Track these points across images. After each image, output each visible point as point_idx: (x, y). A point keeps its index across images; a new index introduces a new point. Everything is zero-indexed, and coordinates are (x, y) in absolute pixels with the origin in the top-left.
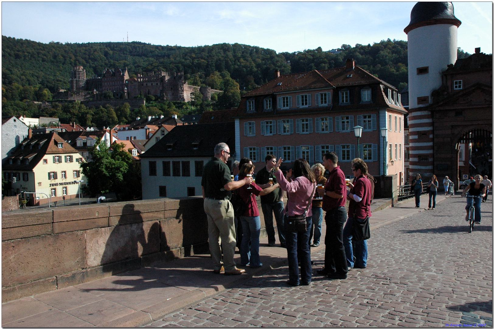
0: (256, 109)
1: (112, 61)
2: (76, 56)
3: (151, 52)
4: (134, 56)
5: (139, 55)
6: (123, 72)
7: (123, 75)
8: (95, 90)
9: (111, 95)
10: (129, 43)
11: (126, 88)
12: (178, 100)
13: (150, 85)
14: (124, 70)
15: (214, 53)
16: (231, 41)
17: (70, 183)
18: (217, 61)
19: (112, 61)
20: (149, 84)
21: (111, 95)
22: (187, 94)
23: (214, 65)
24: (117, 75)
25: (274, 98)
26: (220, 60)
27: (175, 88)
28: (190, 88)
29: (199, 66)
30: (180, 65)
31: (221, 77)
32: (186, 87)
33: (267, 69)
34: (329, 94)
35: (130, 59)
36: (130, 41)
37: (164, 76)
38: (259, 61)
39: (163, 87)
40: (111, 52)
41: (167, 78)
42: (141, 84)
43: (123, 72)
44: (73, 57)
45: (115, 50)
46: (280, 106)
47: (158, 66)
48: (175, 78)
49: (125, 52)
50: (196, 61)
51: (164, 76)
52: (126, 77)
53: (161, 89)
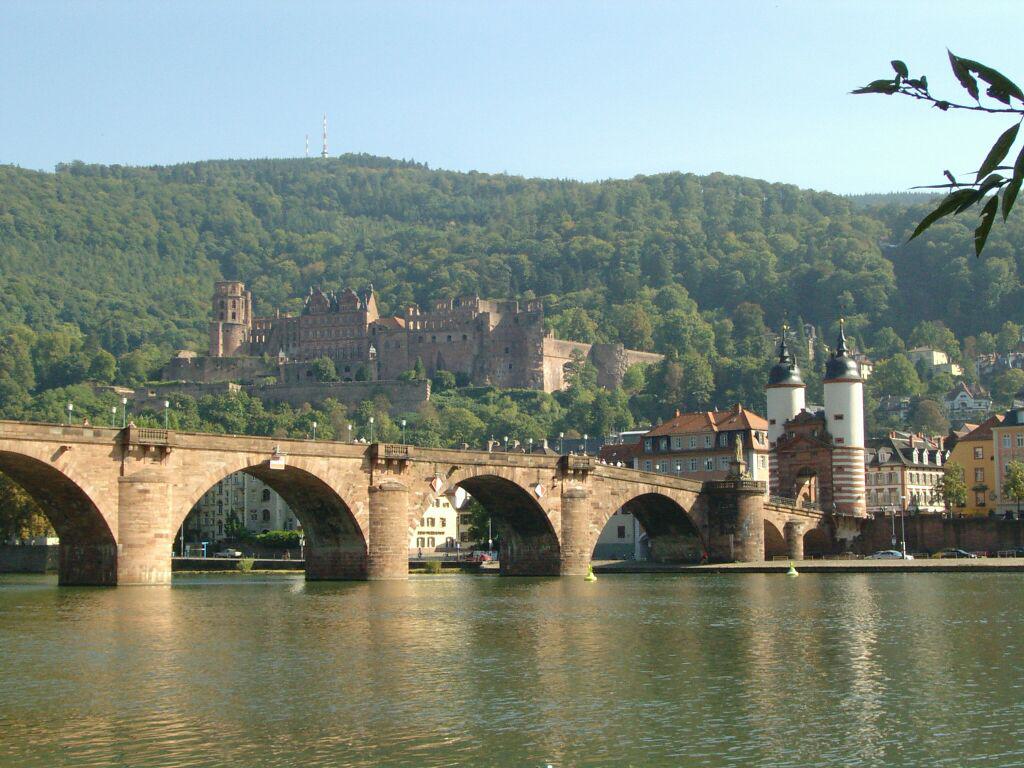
0: (653, 449)
1: (281, 232)
2: (160, 217)
3: (417, 199)
4: (357, 214)
5: (370, 213)
6: (363, 301)
7: (364, 309)
8: (282, 354)
9: (330, 366)
10: (332, 162)
11: (373, 350)
12: (525, 387)
13: (445, 340)
14: (364, 294)
15: (638, 213)
16: (699, 163)
17: (436, 533)
18: (648, 243)
19: (281, 232)
20: (441, 338)
21: (330, 366)
22: (553, 369)
23: (637, 257)
24: (345, 308)
25: (668, 438)
26: (657, 239)
27: (520, 351)
28: (561, 348)
29: (588, 261)
30: (524, 258)
31: (655, 308)
32: (549, 345)
33: (814, 275)
34: (712, 438)
35: (341, 222)
36: (335, 152)
37: (486, 315)
38: (791, 243)
39: (481, 345)
40: (276, 200)
41: (494, 321)
42: (416, 338)
43: (363, 301)
44: (155, 226)
45: (292, 193)
46: (675, 447)
47: (449, 262)
48: (516, 321)
49: (326, 200)
50: (576, 243)
51: (486, 315)
52: (372, 316)
53: (475, 351)
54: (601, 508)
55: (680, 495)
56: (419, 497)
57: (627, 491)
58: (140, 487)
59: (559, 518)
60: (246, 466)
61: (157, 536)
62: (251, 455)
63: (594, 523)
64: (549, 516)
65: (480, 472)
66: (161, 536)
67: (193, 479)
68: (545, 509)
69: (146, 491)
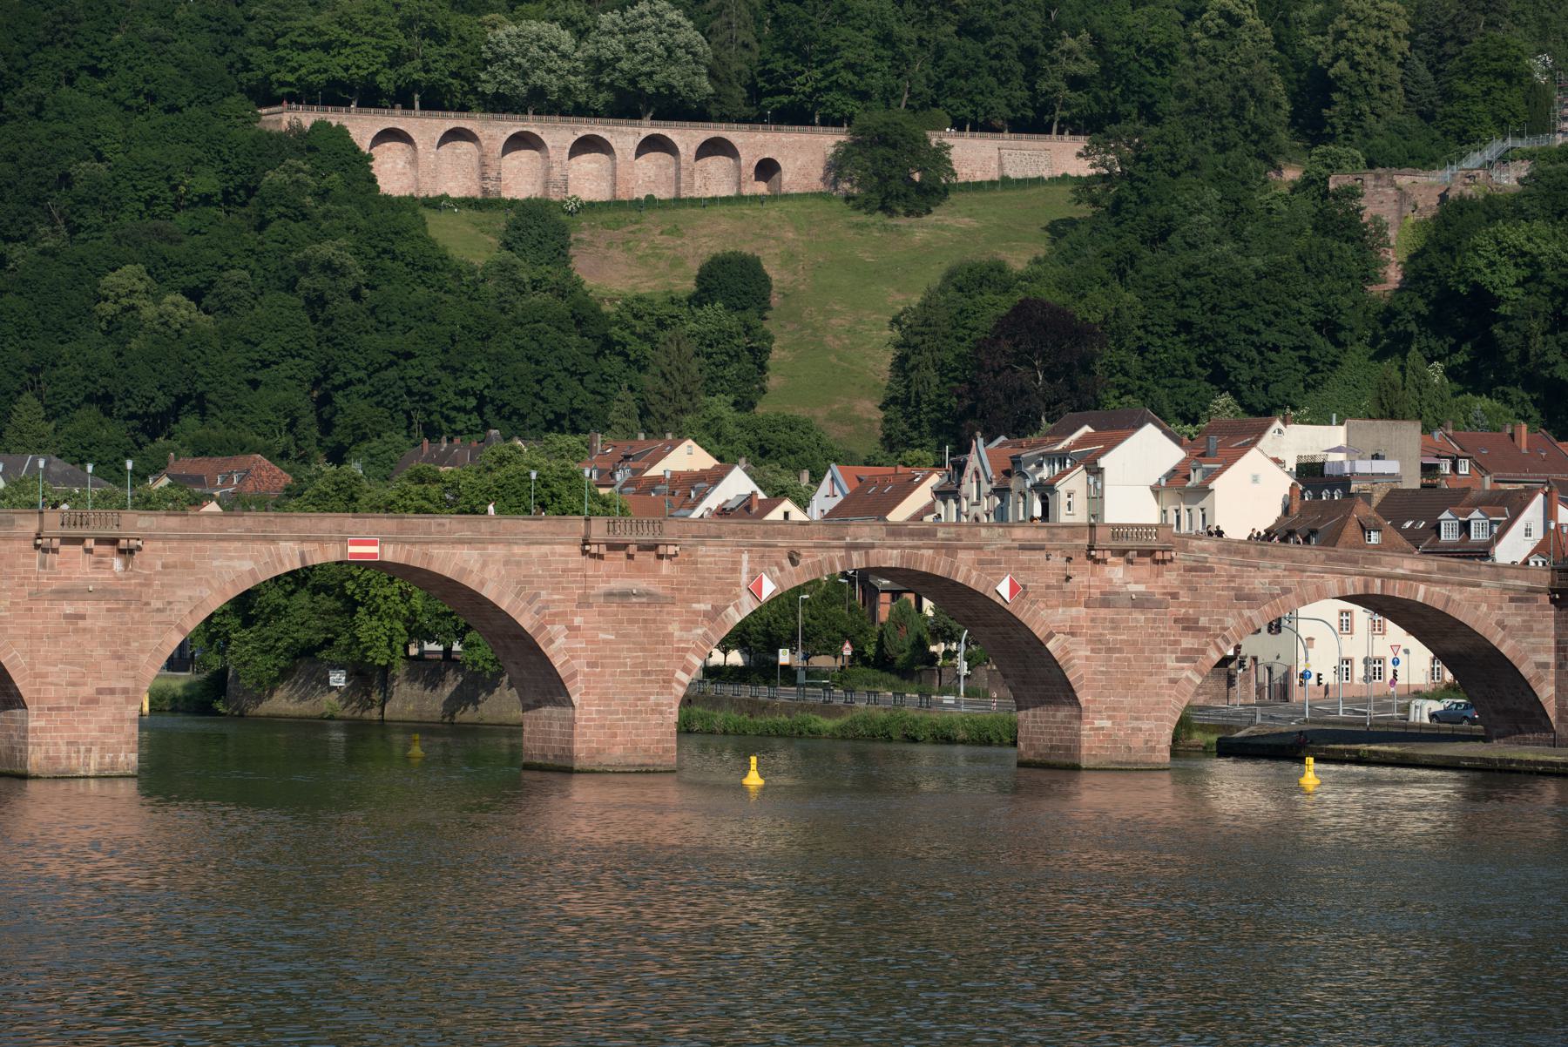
54: (1204, 629)
55: (1456, 596)
56: (706, 614)
57: (1286, 591)
58: (69, 610)
59: (1084, 652)
60: (298, 565)
61: (100, 691)
62: (307, 547)
63: (1178, 660)
64: (1050, 645)
65: (858, 561)
66: (112, 691)
67: (182, 593)
68: (1040, 633)
69: (83, 617)
